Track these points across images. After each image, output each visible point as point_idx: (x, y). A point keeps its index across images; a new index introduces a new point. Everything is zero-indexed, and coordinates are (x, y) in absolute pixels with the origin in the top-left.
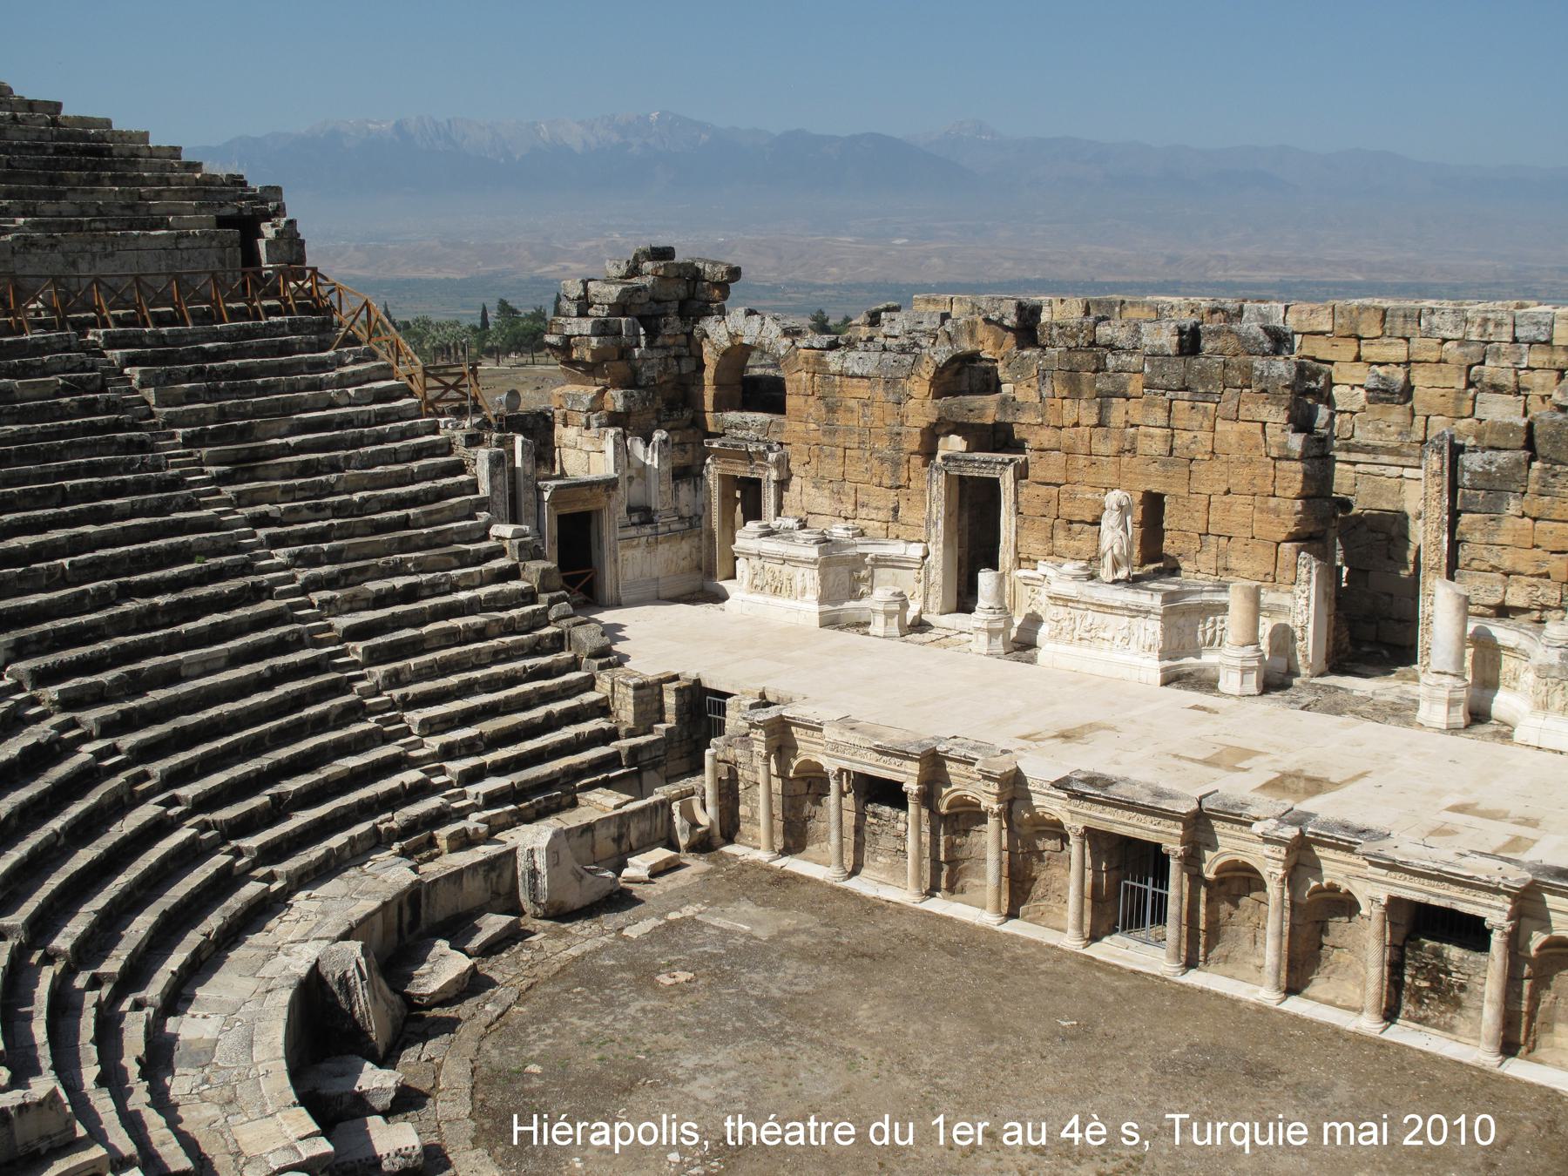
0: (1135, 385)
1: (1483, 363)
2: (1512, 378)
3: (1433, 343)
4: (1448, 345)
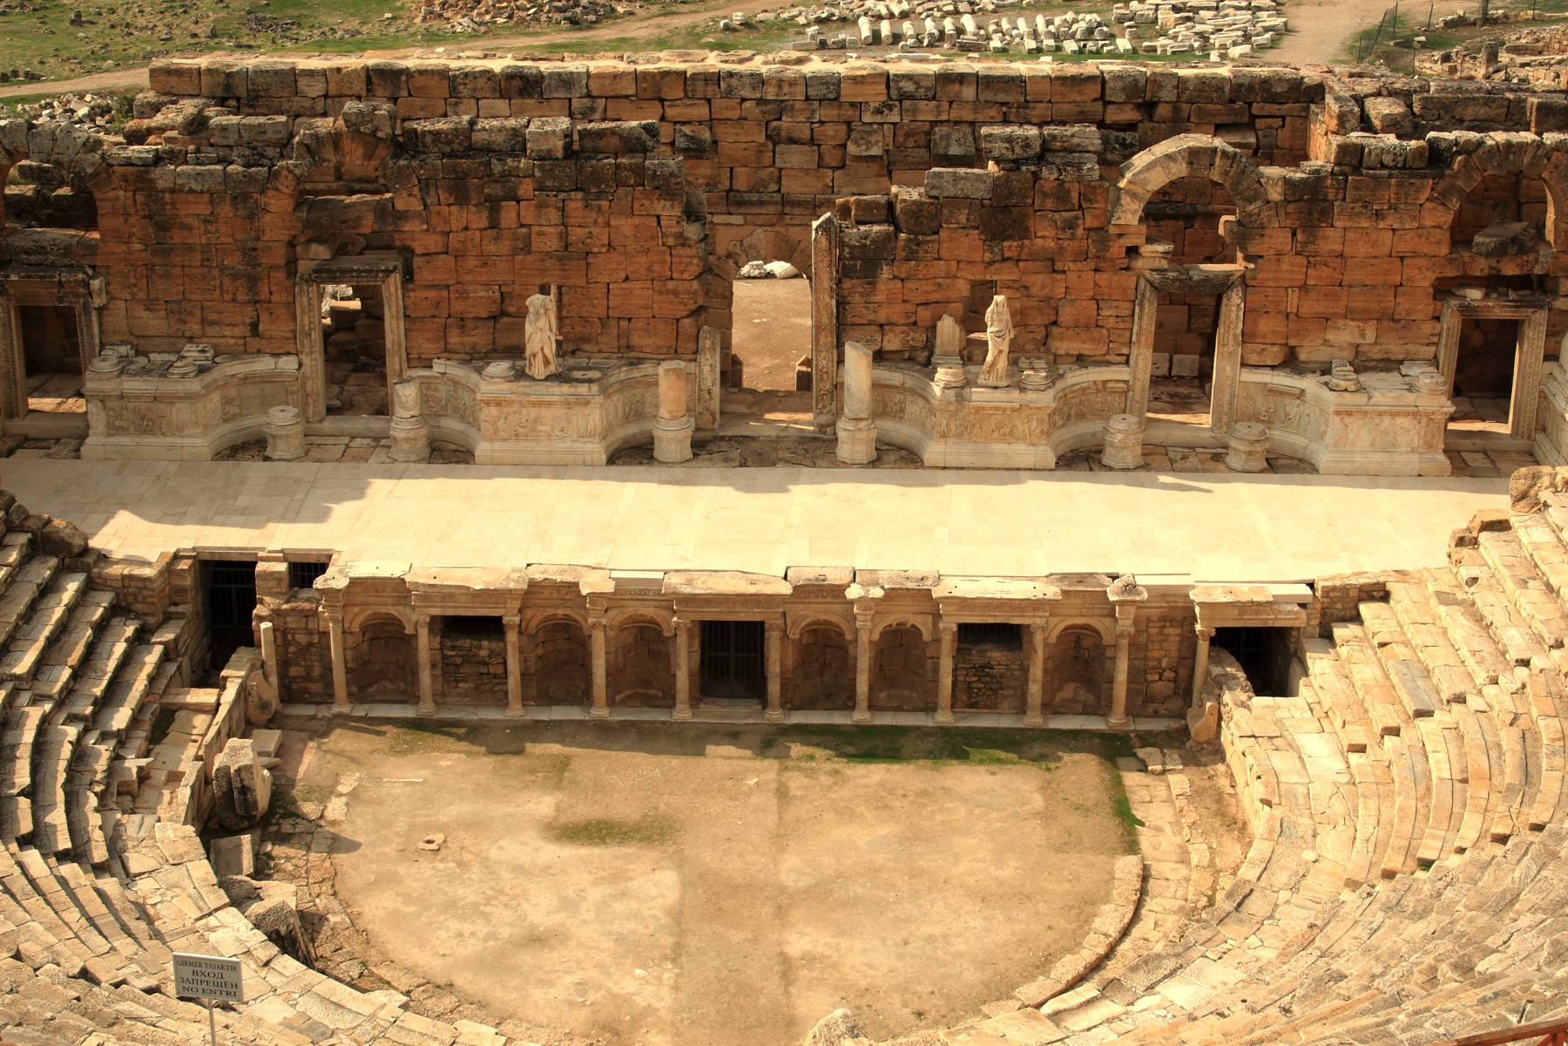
0: (526, 188)
1: (780, 119)
2: (808, 132)
3: (734, 102)
4: (747, 104)
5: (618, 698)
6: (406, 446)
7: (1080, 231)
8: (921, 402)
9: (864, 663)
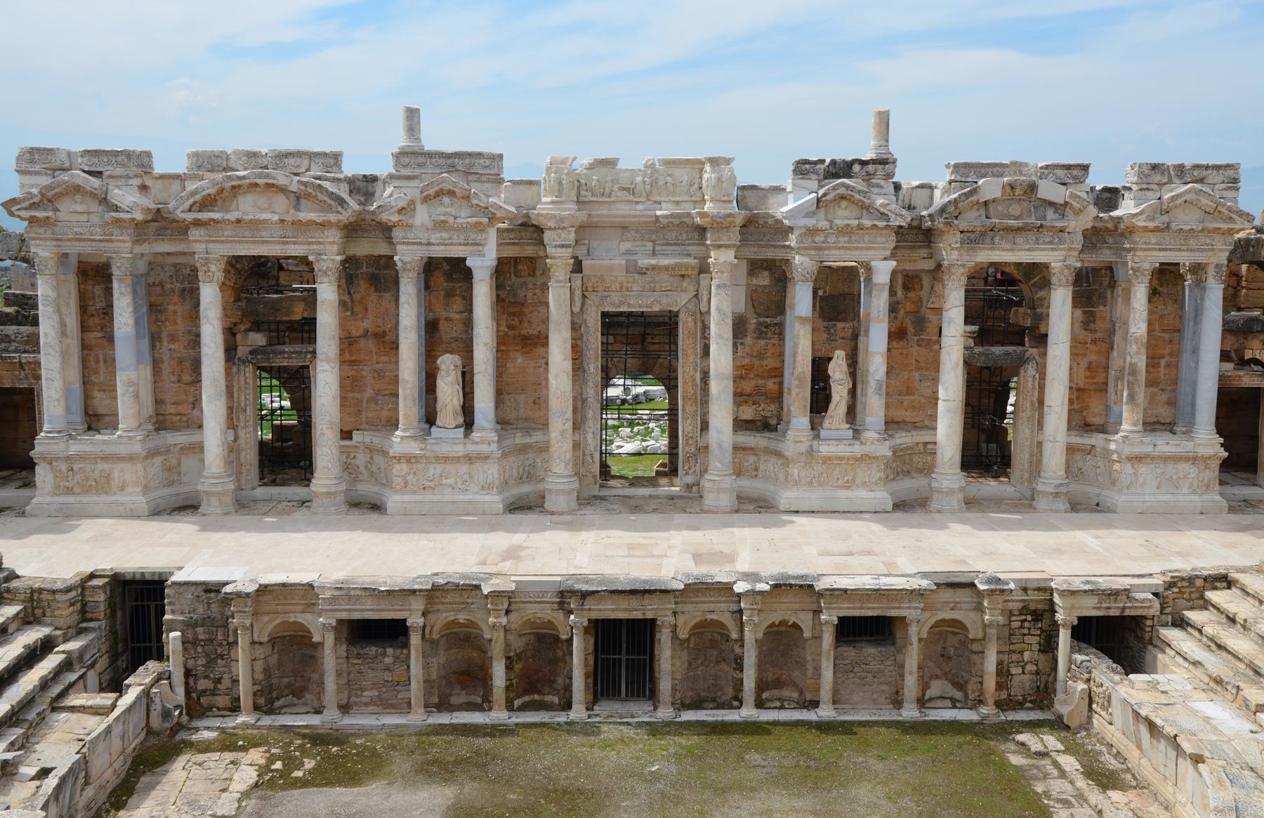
5: (517, 703)
6: (326, 500)
7: (902, 313)
8: (774, 460)
9: (750, 659)
